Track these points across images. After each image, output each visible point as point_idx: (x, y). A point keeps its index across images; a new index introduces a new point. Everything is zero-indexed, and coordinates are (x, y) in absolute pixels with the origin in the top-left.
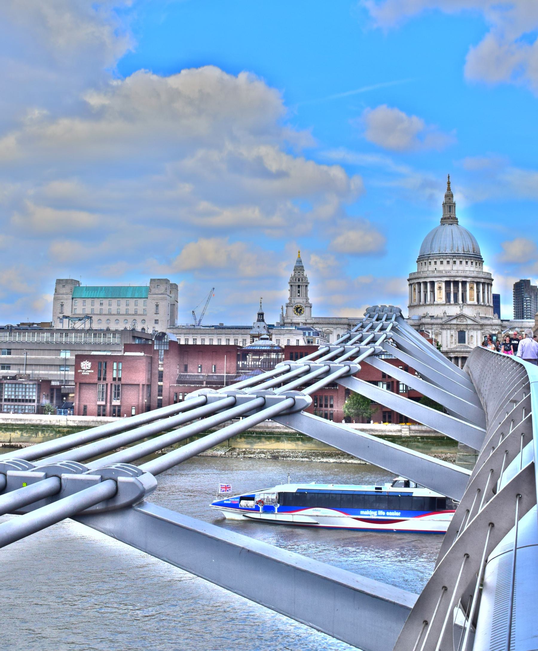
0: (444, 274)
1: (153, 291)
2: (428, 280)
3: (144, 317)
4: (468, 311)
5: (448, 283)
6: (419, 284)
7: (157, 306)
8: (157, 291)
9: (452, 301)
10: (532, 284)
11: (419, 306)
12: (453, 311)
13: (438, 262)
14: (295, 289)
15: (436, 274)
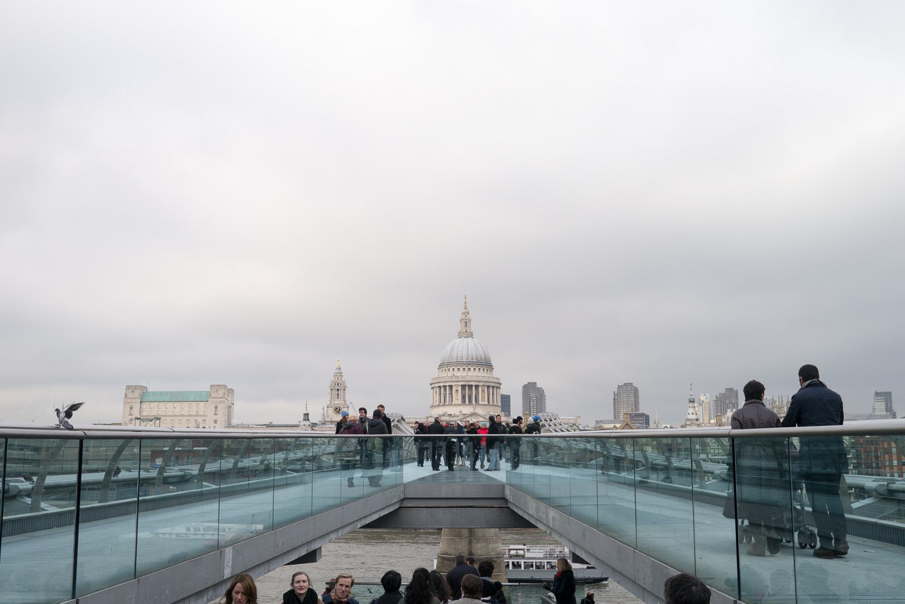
0: (461, 379)
1: (213, 395)
2: (447, 384)
3: (203, 418)
4: (480, 411)
5: (463, 387)
6: (440, 387)
7: (216, 408)
8: (216, 395)
9: (467, 402)
10: (538, 386)
11: (439, 405)
12: (467, 410)
13: (456, 369)
14: (335, 392)
15: (454, 379)
